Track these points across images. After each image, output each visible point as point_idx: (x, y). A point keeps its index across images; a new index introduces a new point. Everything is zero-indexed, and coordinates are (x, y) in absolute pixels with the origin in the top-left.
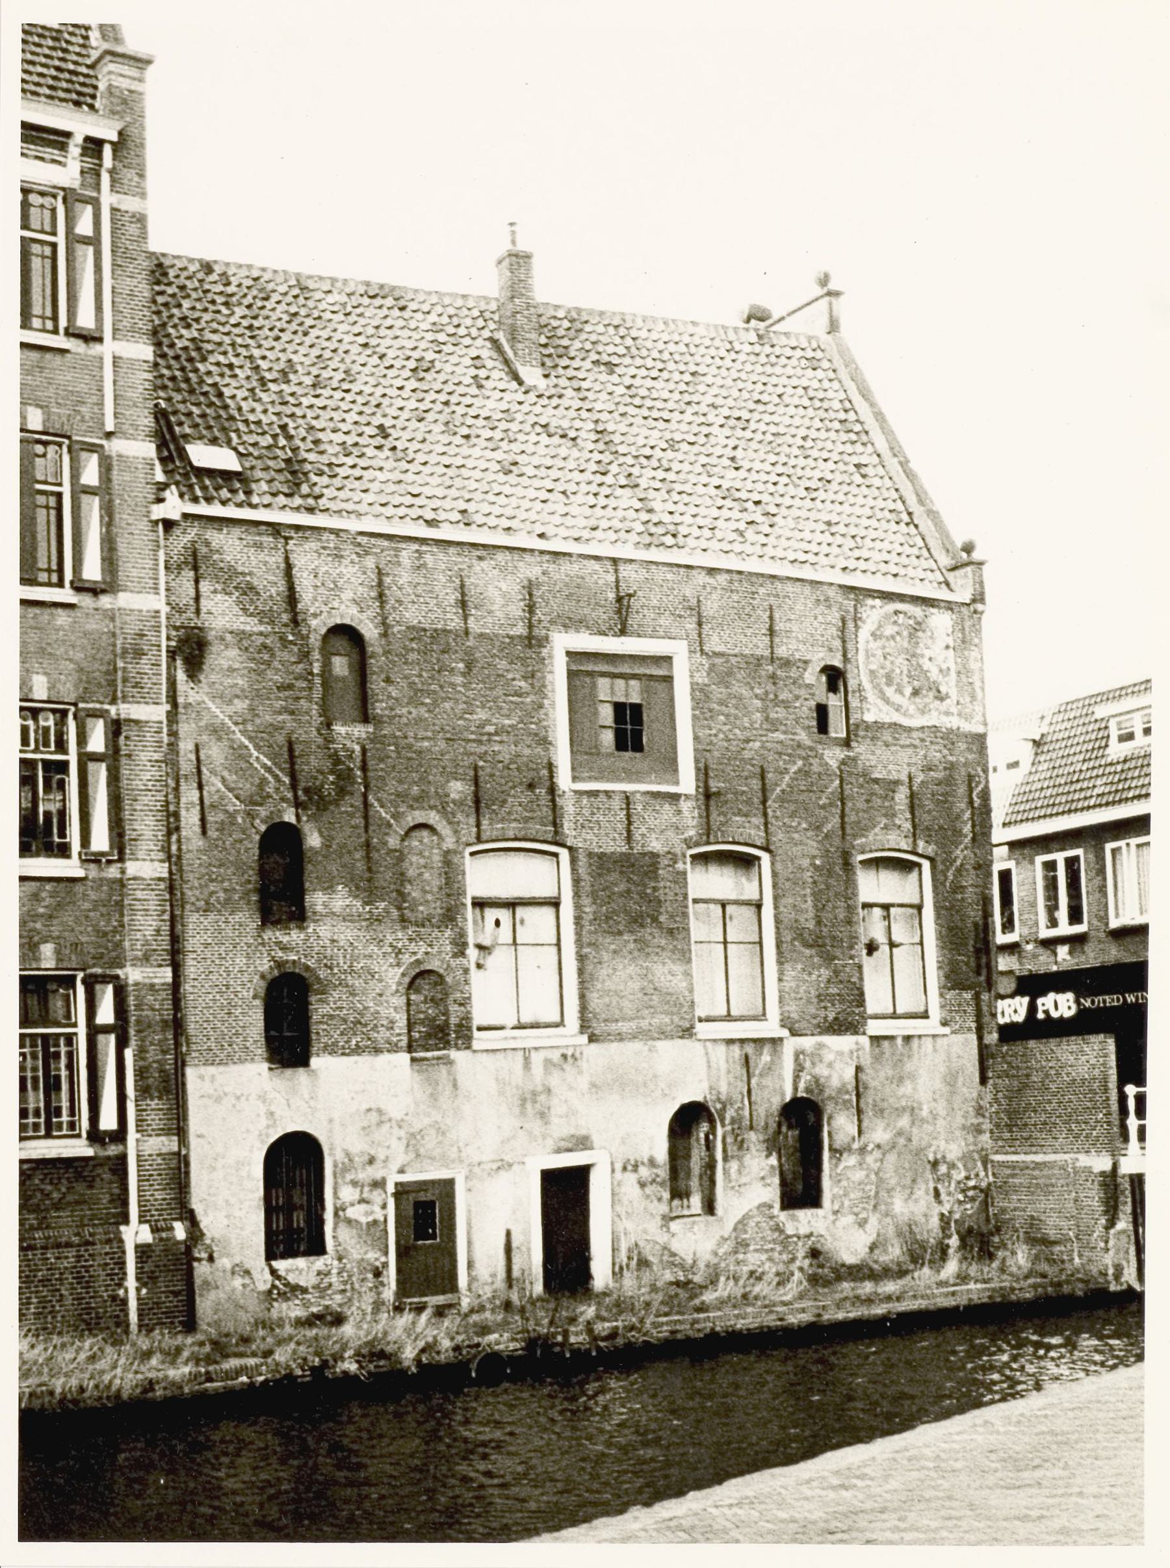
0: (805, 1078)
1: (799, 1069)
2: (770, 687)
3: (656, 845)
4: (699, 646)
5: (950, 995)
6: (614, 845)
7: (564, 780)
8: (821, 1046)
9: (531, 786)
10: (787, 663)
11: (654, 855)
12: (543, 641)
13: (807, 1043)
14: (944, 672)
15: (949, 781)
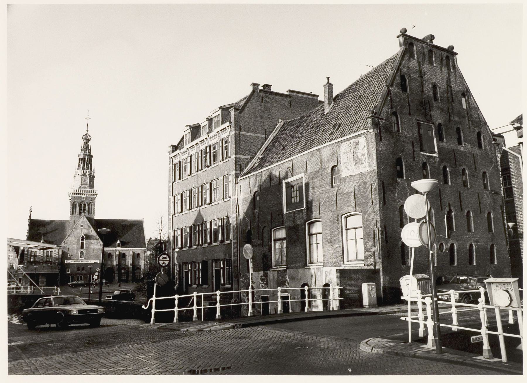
0: (328, 279)
1: (327, 276)
2: (321, 177)
3: (299, 223)
4: (306, 172)
5: (367, 253)
6: (292, 224)
7: (285, 212)
8: (331, 270)
9: (279, 215)
10: (325, 169)
11: (298, 225)
12: (282, 183)
13: (328, 269)
14: (363, 155)
15: (365, 188)
